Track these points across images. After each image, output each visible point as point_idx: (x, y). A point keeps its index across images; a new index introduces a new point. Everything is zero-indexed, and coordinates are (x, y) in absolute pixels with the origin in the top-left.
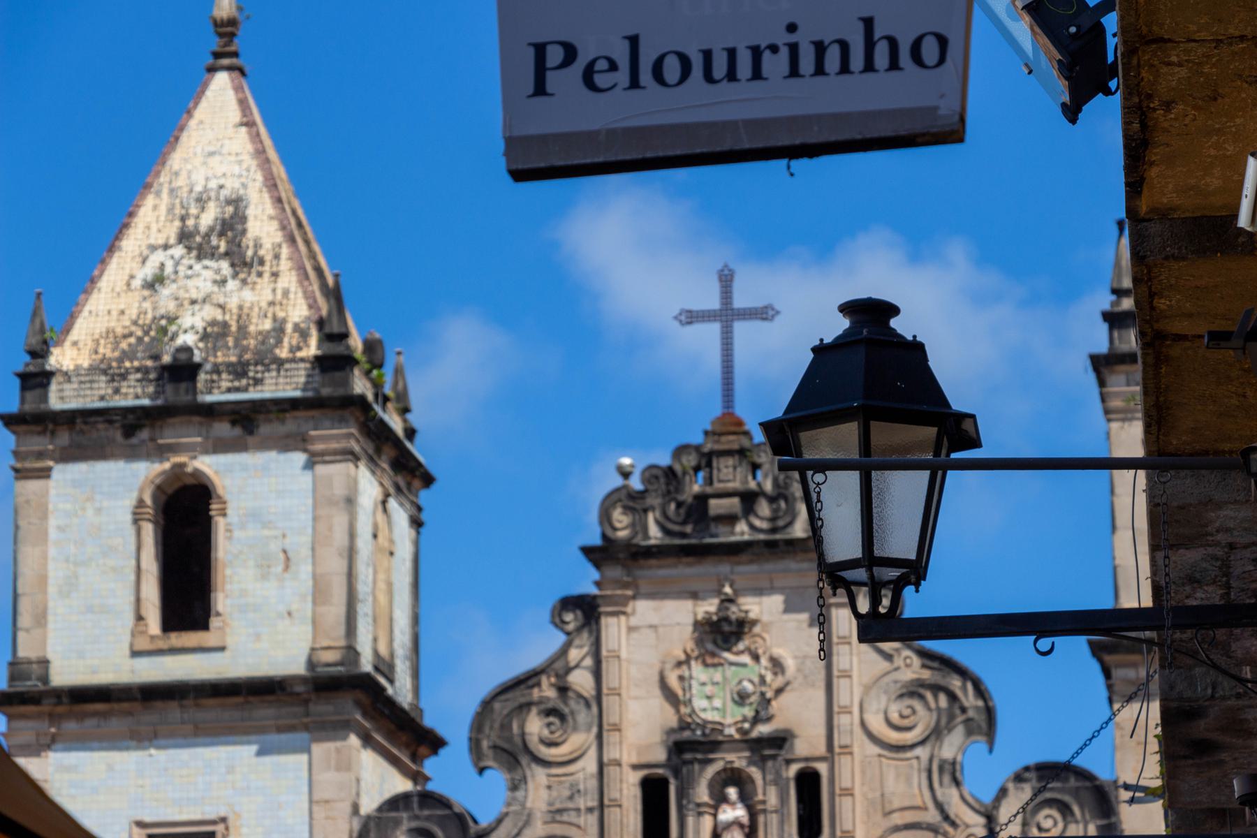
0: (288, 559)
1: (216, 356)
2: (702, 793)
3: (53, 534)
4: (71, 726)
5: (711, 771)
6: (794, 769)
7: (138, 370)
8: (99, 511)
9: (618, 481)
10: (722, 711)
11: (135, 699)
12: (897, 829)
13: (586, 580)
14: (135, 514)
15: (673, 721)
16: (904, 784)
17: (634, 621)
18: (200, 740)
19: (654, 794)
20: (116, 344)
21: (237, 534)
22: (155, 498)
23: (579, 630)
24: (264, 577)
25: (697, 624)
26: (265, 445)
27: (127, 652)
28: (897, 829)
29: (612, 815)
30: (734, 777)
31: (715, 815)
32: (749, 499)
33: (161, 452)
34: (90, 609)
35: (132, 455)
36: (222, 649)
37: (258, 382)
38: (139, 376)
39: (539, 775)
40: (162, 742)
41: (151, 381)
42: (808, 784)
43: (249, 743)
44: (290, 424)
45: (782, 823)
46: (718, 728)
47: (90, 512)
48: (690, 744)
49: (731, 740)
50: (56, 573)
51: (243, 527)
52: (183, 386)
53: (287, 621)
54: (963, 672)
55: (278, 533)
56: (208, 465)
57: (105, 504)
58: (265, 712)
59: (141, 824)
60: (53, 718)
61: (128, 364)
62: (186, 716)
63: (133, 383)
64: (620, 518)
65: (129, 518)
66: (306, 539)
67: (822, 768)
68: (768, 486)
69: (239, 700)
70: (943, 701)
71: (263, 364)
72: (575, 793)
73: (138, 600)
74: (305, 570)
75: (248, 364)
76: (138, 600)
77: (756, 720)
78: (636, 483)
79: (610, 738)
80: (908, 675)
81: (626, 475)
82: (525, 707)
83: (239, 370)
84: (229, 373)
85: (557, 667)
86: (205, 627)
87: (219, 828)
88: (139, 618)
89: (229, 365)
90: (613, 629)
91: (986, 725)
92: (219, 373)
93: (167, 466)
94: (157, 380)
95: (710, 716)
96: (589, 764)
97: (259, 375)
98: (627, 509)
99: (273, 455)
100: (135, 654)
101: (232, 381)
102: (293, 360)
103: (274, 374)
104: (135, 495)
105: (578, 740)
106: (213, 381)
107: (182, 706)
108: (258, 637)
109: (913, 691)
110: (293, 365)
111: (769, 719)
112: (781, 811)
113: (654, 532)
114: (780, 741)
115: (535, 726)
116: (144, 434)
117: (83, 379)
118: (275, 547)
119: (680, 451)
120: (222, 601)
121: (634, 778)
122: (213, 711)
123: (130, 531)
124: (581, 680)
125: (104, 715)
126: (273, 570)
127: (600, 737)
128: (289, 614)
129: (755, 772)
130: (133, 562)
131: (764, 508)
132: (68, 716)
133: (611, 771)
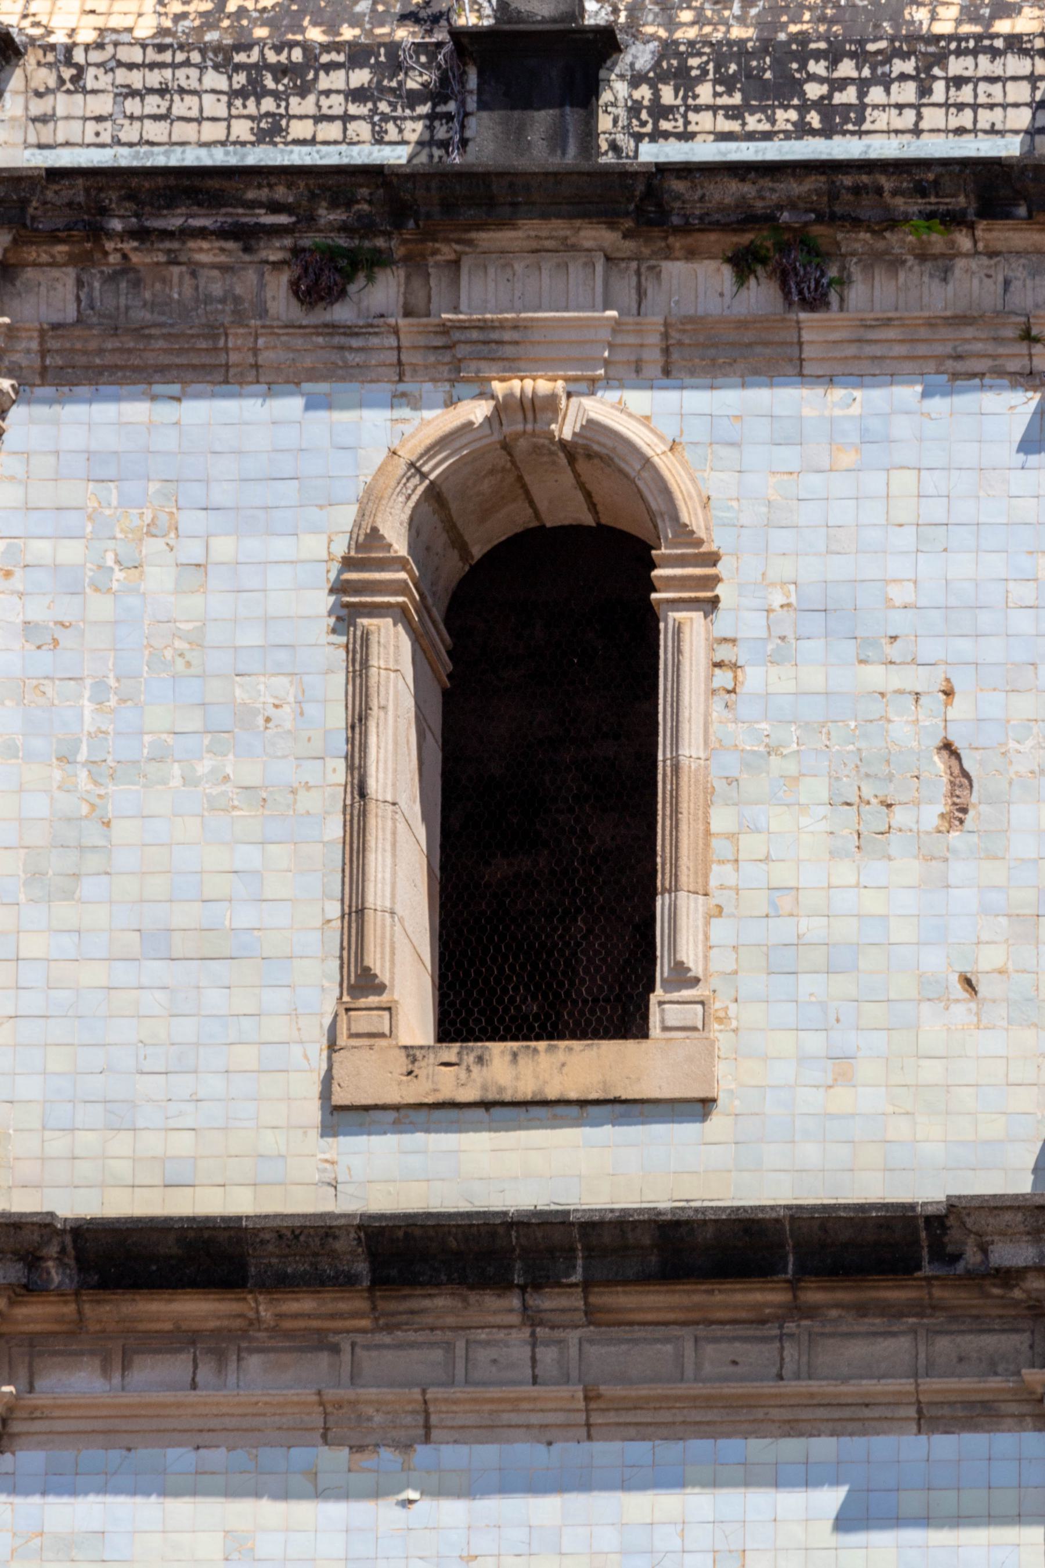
1: (672, 24)
4: (76, 1383)
7: (357, 55)
11: (346, 1281)
14: (339, 588)
18: (605, 1451)
21: (753, 678)
22: (415, 526)
26: (863, 363)
27: (313, 1112)
33: (459, 354)
34: (157, 944)
35: (334, 367)
36: (702, 1107)
37: (835, 120)
38: (361, 77)
40: (451, 1454)
41: (413, 99)
43: (809, 1482)
44: (971, 284)
47: (159, 578)
51: (780, 652)
52: (542, 119)
53: (962, 1011)
55: (927, 680)
56: (639, 415)
57: (223, 547)
58: (870, 1355)
61: (315, 35)
62: (548, 1355)
63: (336, 104)
65: (322, 602)
69: (769, 1296)
71: (860, 57)
73: (356, 914)
75: (801, 50)
76: (356, 914)
83: (765, 75)
84: (729, 84)
88: (361, 982)
89: (724, 52)
92: (684, 80)
93: (478, 411)
94: (437, 94)
97: (849, 96)
99: (908, 393)
100: (342, 1116)
101: (734, 113)
102: (981, 46)
103: (907, 92)
104: (346, 516)
106: (660, 111)
107: (532, 1319)
108: (842, 1066)
110: (985, 65)
116: (382, 293)
117: (136, 79)
118: (912, 732)
120: (692, 928)
122: (657, 1337)
123: (329, 654)
125: (217, 1346)
126: (901, 817)
128: (968, 983)
130: (338, 772)
132: (68, 1342)
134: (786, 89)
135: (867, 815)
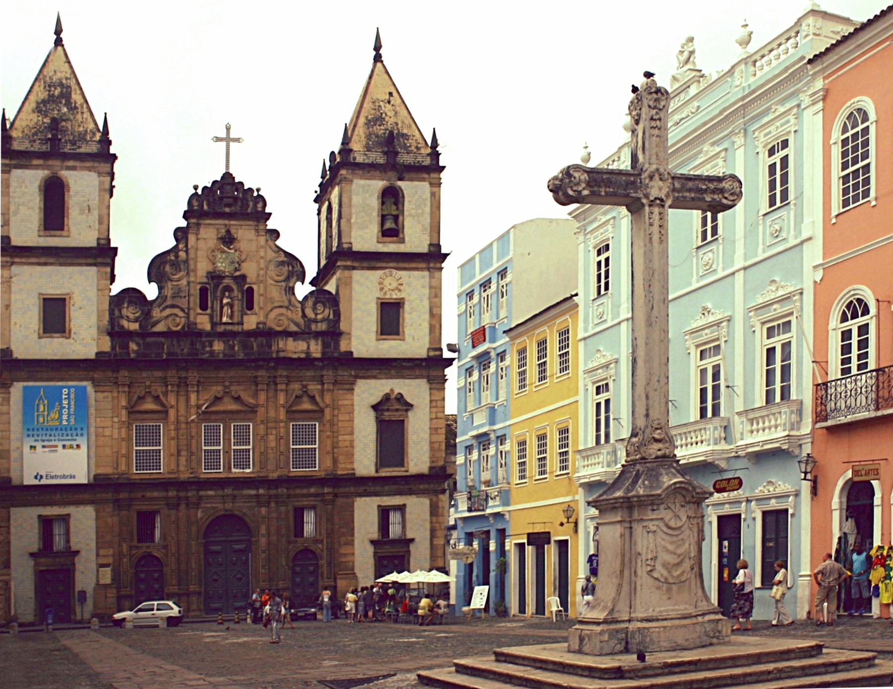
0: (89, 210)
2: (219, 294)
3: (11, 194)
4: (17, 260)
5: (221, 287)
6: (247, 286)
8: (26, 187)
9: (194, 191)
10: (225, 267)
12: (276, 307)
13: (184, 223)
15: (210, 269)
16: (276, 294)
17: (199, 236)
19: (203, 292)
20: (31, 129)
23: (182, 238)
24: (82, 214)
25: (218, 239)
28: (276, 307)
29: (192, 299)
30: (228, 289)
31: (221, 301)
32: (236, 199)
36: (68, 236)
37: (80, 147)
39: (170, 284)
42: (250, 291)
45: (242, 304)
46: (224, 272)
48: (215, 277)
49: (228, 276)
50: (12, 208)
54: (297, 259)
56: (65, 174)
59: (40, 294)
60: (11, 256)
64: (195, 203)
66: (96, 201)
67: (255, 287)
68: (241, 195)
70: (290, 268)
72: (180, 290)
74: (96, 213)
77: (236, 270)
78: (199, 191)
79: (192, 274)
80: (280, 259)
81: (196, 188)
82: (165, 263)
83: (73, 143)
85: (175, 249)
86: (62, 229)
87: (67, 297)
90: (192, 239)
91: (302, 278)
95: (222, 269)
96: (184, 282)
98: (197, 200)
105: (182, 273)
108: (80, 234)
109: (282, 263)
111: (239, 270)
112: (242, 300)
113: (205, 207)
114: (243, 277)
115: (168, 268)
118: (85, 205)
119: (215, 182)
121: (199, 287)
124: (182, 254)
127: (188, 274)
129: (235, 287)
131: (239, 203)
133: (192, 285)
134: (75, 144)
135: (82, 212)
